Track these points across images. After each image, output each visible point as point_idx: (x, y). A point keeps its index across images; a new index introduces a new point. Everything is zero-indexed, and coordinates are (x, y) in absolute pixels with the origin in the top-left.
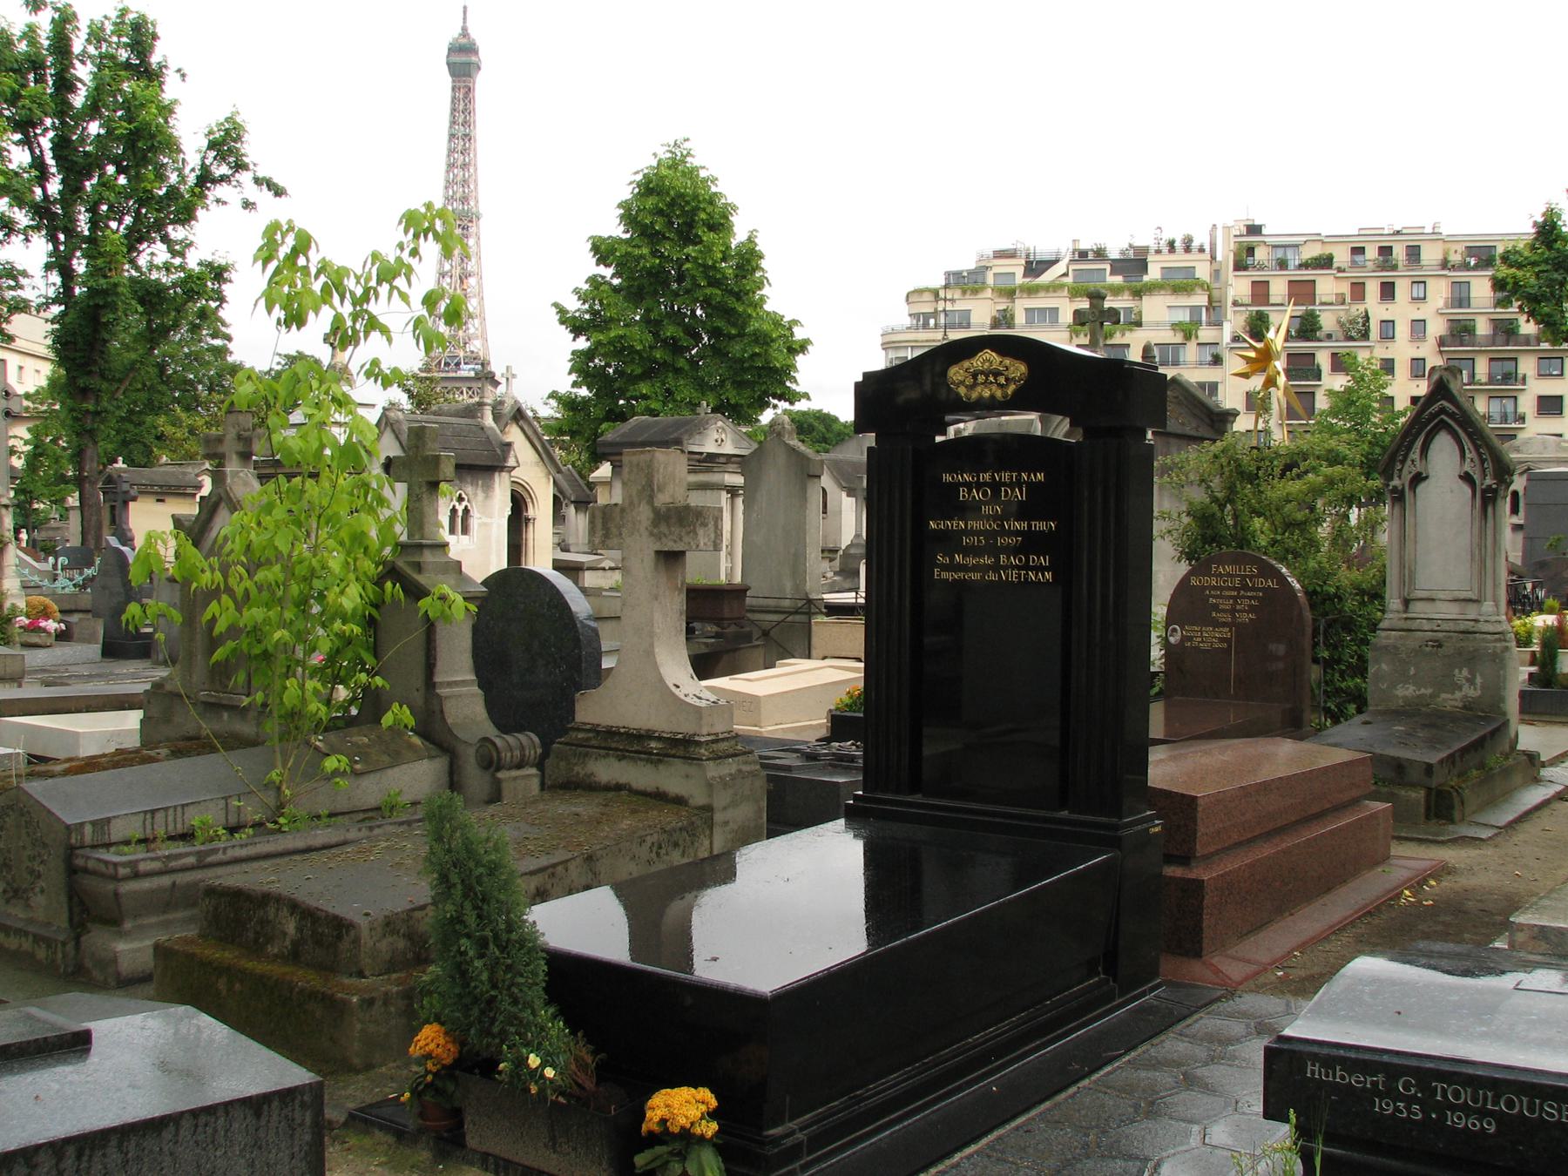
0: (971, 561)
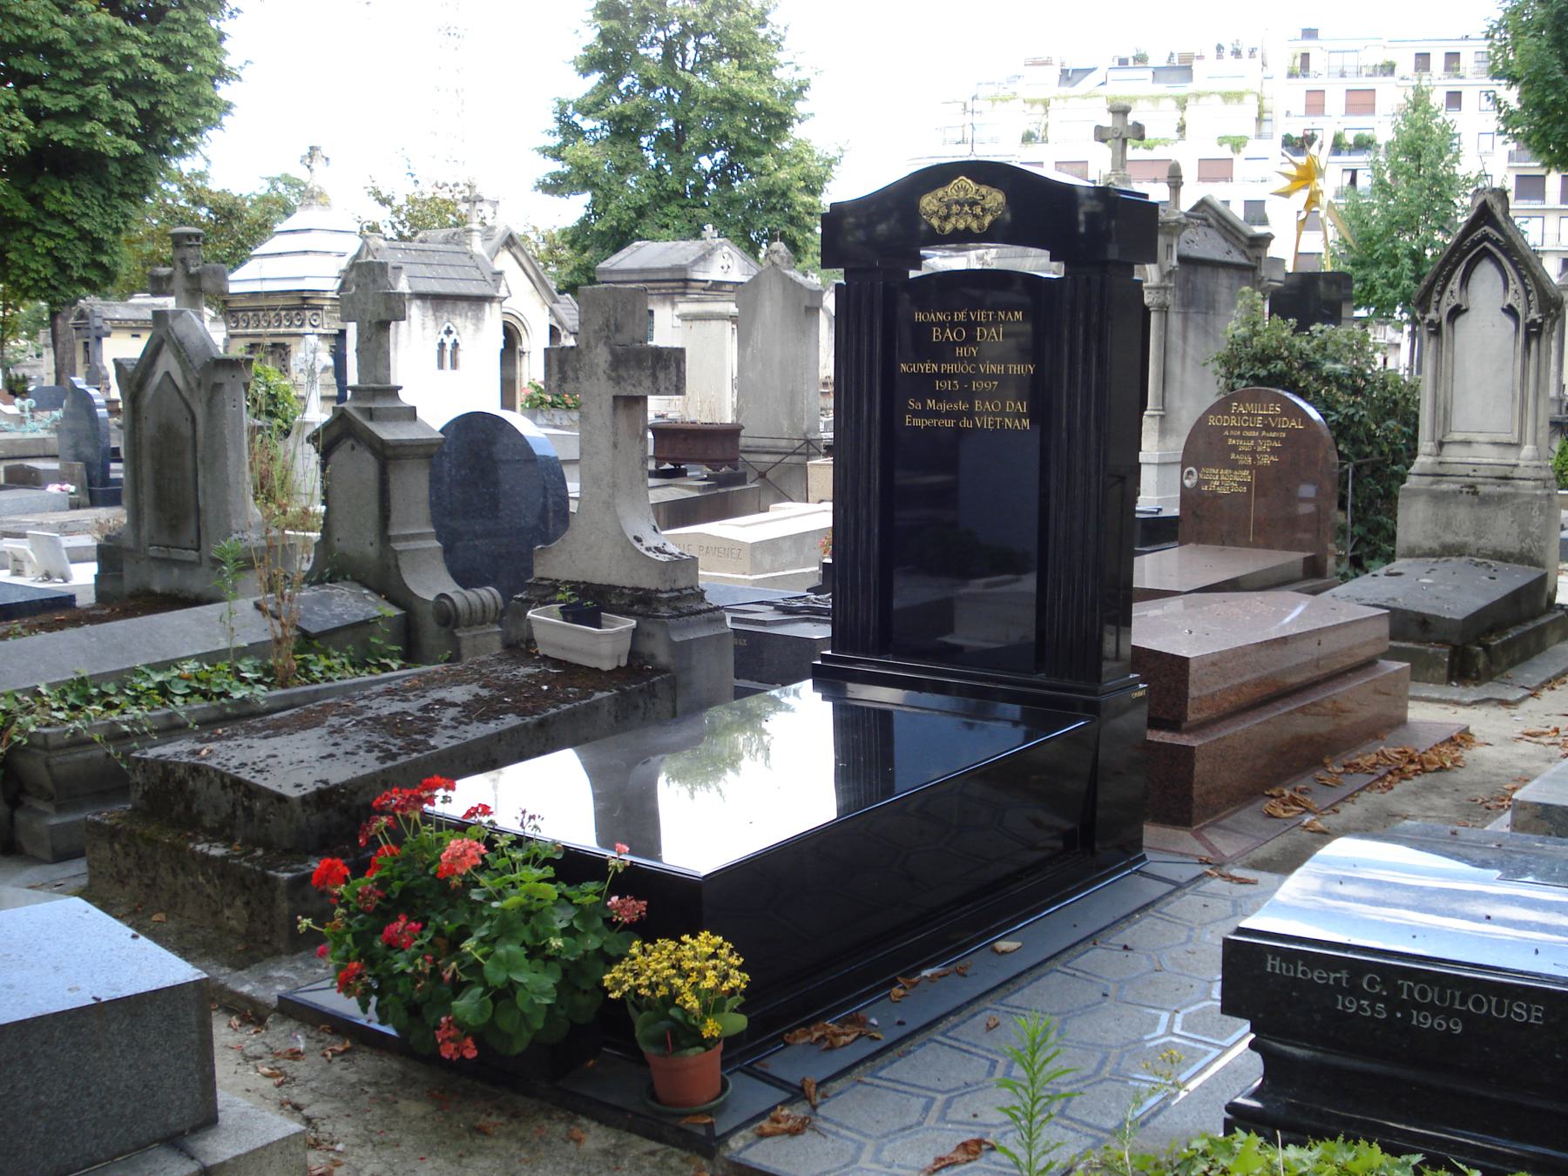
0: (944, 407)
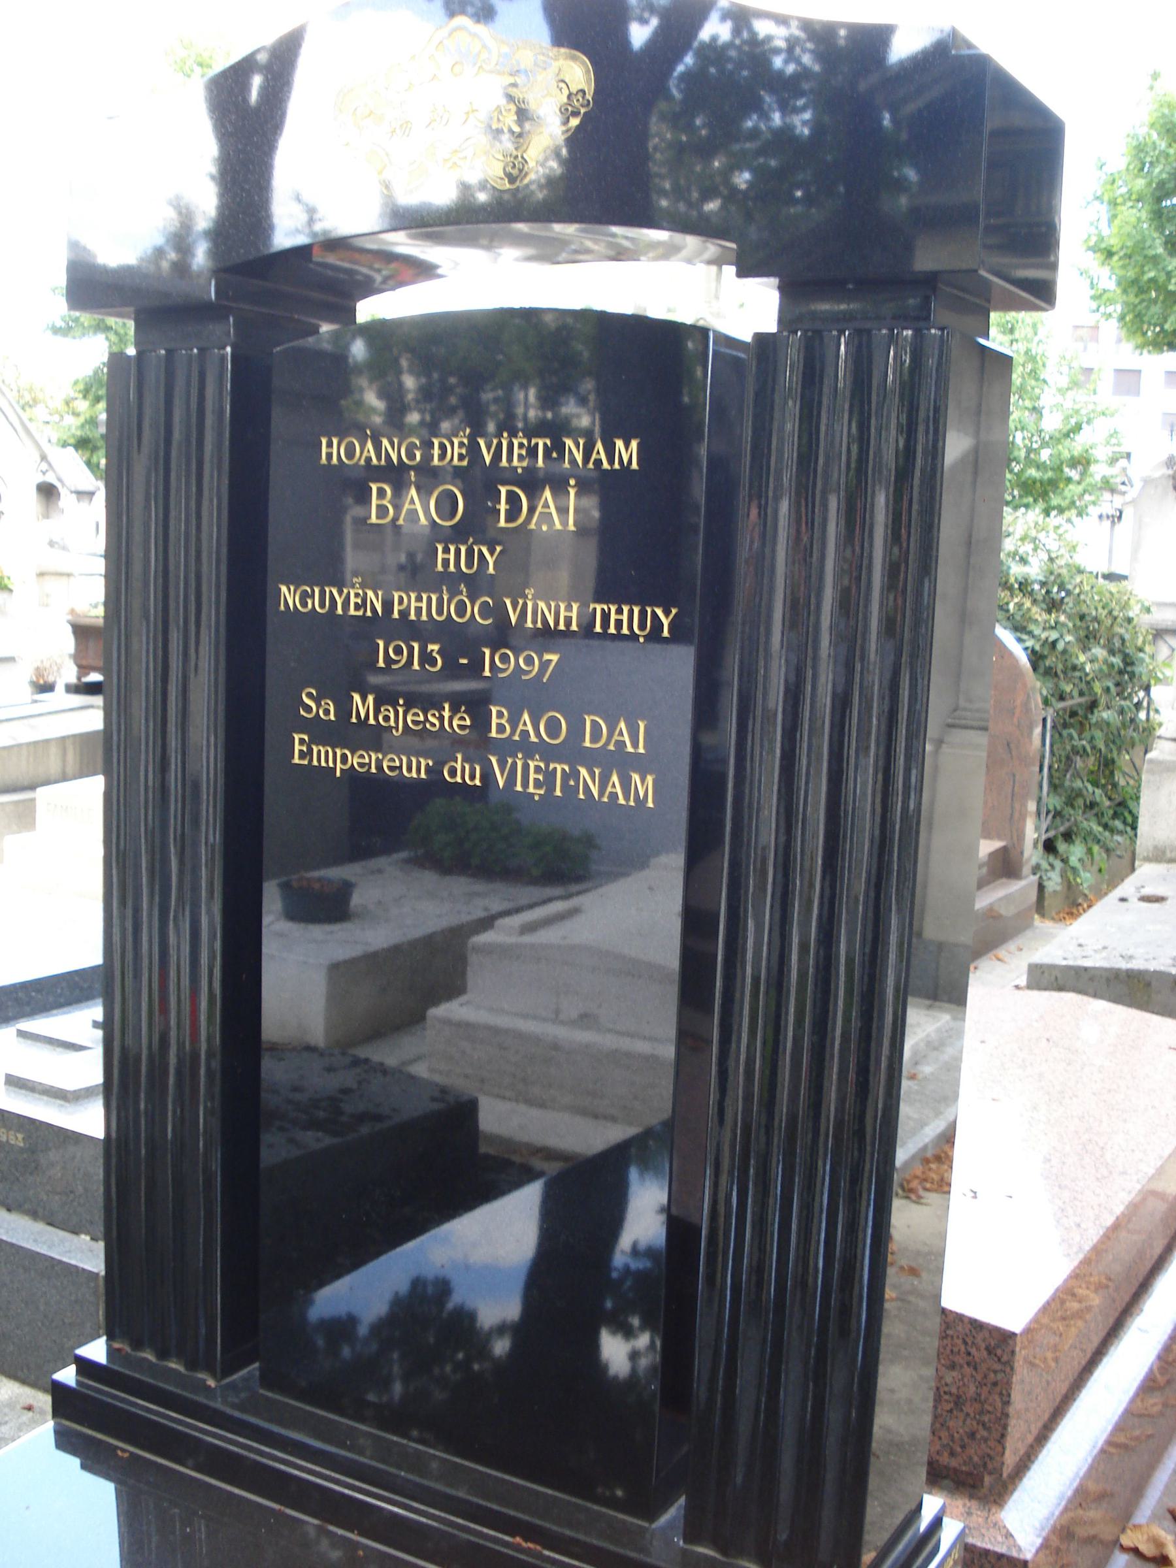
0: (398, 719)
